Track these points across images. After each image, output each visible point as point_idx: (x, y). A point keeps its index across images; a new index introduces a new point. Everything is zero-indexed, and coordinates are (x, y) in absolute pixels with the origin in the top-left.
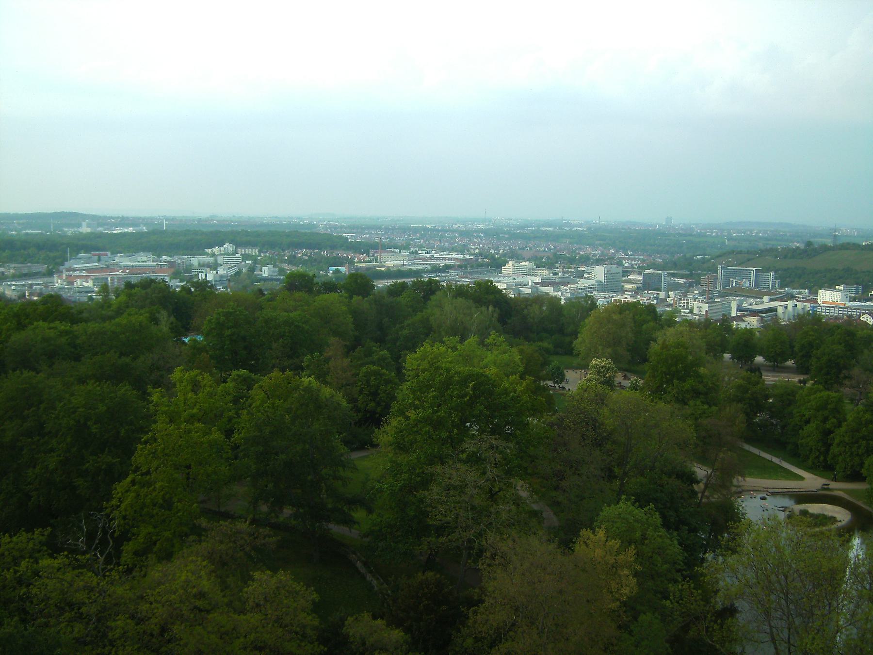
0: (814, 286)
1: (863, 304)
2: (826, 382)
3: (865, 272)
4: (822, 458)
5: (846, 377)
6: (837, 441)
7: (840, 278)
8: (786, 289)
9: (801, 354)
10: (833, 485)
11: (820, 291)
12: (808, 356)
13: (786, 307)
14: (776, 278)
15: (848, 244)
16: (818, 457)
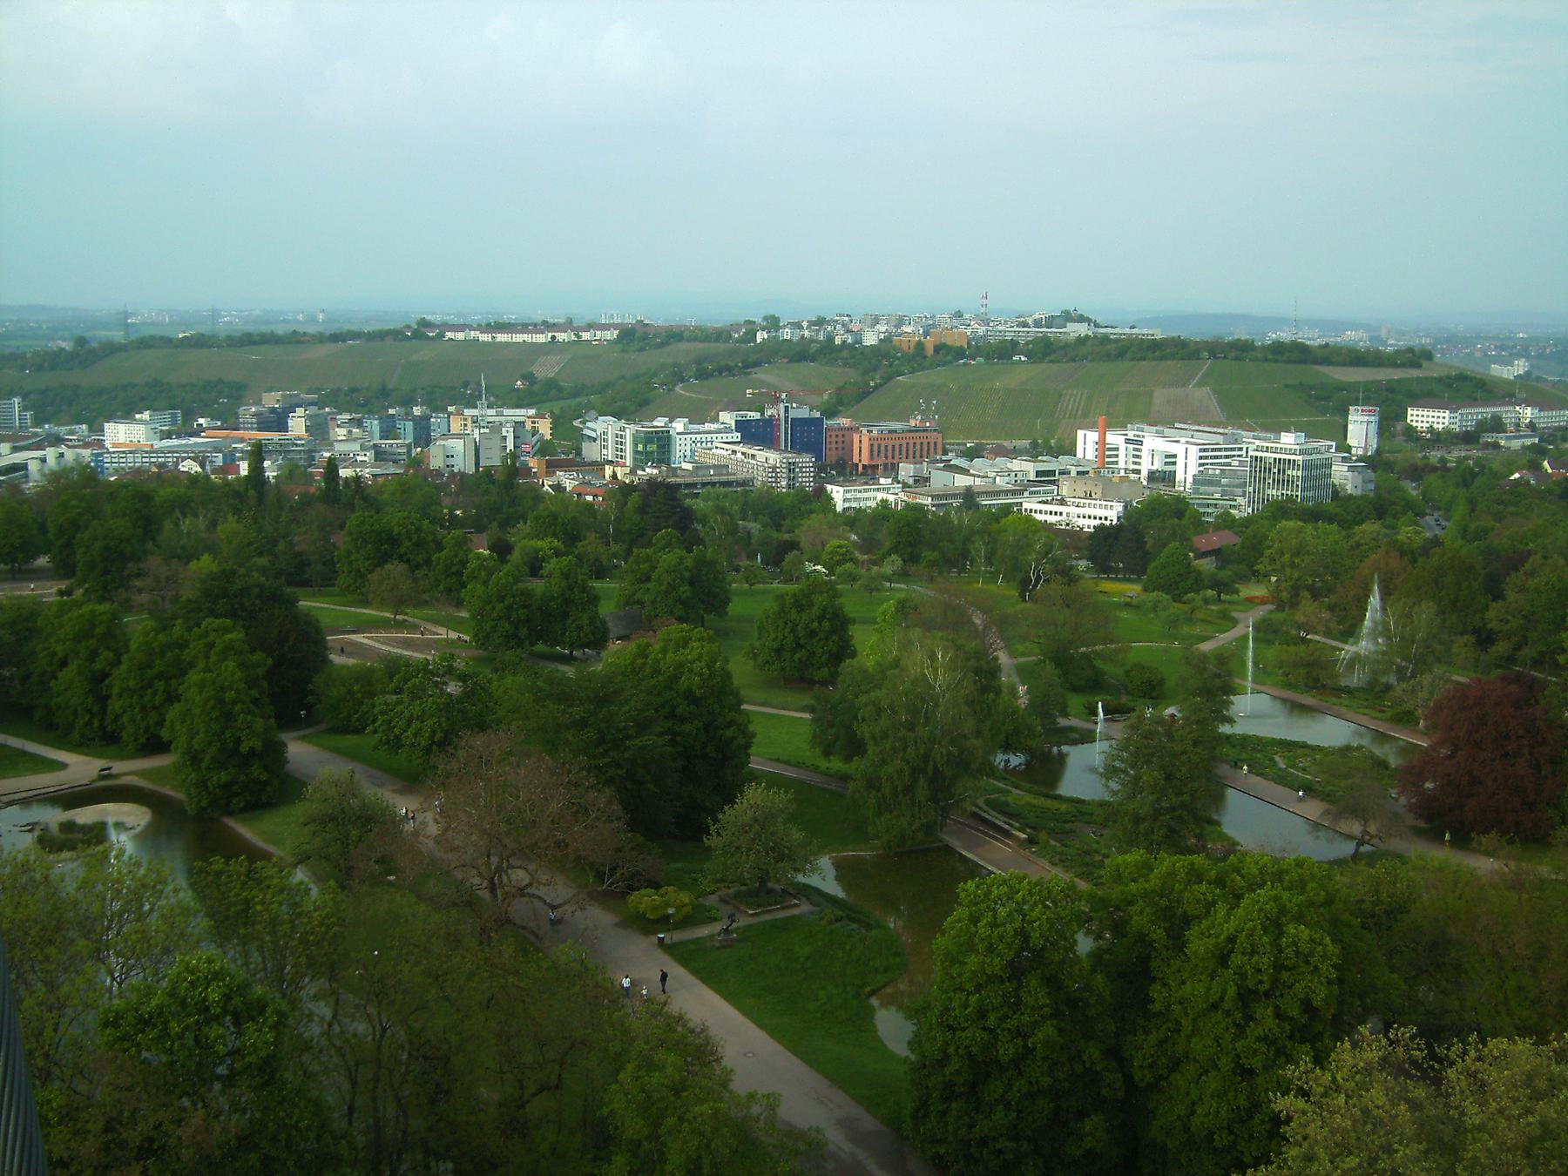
0: (96, 417)
1: (184, 442)
2: (105, 588)
3: (183, 386)
4: (96, 724)
5: (139, 575)
6: (116, 691)
7: (143, 399)
8: (47, 426)
9: (58, 543)
10: (119, 767)
11: (107, 425)
12: (69, 545)
13: (44, 460)
14: (25, 408)
15: (152, 338)
16: (89, 724)
